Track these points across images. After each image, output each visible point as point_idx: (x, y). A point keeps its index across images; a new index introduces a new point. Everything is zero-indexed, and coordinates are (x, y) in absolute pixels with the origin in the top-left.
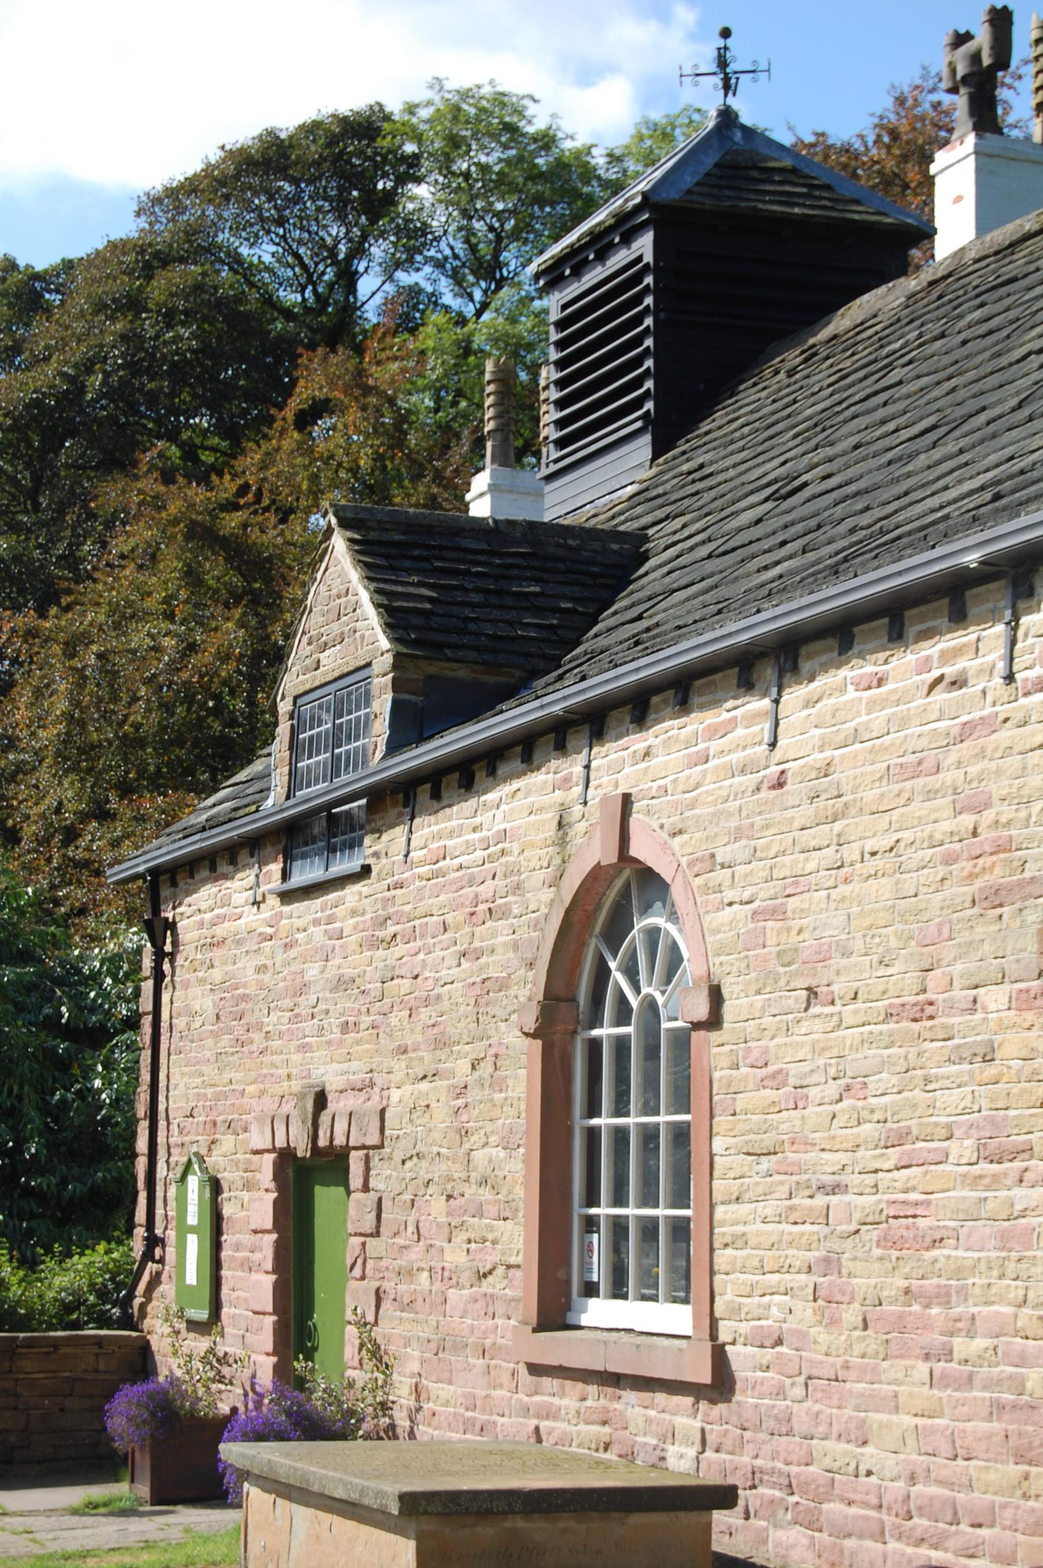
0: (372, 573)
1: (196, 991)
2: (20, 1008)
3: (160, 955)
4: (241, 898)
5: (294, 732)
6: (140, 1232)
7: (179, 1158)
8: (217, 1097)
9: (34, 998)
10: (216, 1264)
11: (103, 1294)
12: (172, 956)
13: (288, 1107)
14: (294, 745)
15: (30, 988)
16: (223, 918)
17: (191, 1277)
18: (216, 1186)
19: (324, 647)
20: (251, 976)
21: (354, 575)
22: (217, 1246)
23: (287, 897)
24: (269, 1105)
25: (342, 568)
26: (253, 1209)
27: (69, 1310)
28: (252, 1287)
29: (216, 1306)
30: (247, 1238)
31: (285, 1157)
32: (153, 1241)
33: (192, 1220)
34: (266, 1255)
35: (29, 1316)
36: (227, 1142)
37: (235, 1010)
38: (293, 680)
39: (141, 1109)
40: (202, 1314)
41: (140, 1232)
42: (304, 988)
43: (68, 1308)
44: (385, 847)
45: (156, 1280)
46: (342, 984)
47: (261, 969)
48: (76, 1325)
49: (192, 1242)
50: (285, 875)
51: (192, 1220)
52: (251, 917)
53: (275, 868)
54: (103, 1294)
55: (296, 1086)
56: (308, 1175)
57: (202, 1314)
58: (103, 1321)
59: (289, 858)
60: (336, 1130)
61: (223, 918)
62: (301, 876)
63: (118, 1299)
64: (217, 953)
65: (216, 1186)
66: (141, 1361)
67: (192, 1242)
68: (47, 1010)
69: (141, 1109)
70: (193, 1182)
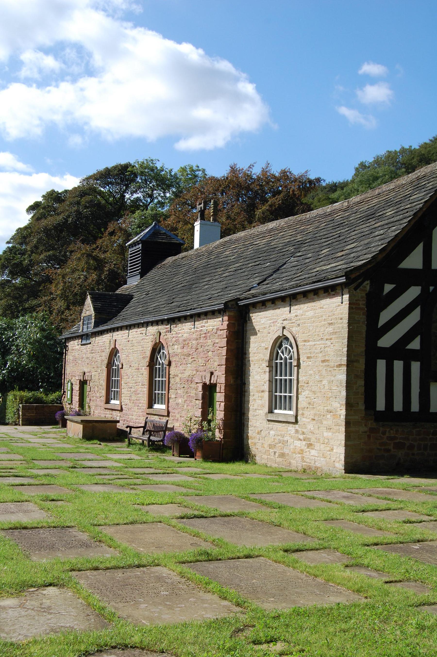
0: (93, 302)
1: (70, 356)
2: (50, 349)
3: (66, 350)
4: (76, 344)
5: (83, 322)
6: (63, 390)
7: (68, 380)
8: (73, 372)
9: (53, 347)
10: (72, 395)
11: (57, 399)
12: (68, 351)
13: (81, 374)
14: (83, 324)
15: (53, 345)
16: (74, 346)
17: (69, 397)
18: (72, 384)
19: (87, 311)
20: (77, 355)
21: (90, 302)
22: (72, 393)
23: (82, 345)
24: (78, 373)
25: (89, 301)
26: (76, 388)
27: (53, 401)
28: (76, 398)
29: (72, 401)
30: (76, 392)
31: (80, 380)
32: (64, 392)
33: (69, 389)
34: (78, 394)
35: (46, 402)
36: (74, 378)
37: (75, 360)
38: (83, 315)
39: (63, 373)
40: (70, 402)
41: (63, 390)
42: (83, 358)
43: (53, 401)
44: (93, 340)
45: (64, 397)
46: (87, 358)
47: (78, 354)
48: (53, 404)
49: (69, 392)
50: (81, 342)
51: (69, 389)
52: (77, 347)
53: (80, 340)
54: (57, 399)
55: (82, 371)
56: (83, 383)
57: (70, 402)
58: (57, 403)
59: (82, 339)
60: (86, 378)
61: (74, 346)
62: (84, 342)
63: (59, 400)
64: (73, 351)
65: (72, 384)
66: (62, 408)
67: (69, 392)
68: (56, 349)
69: (63, 373)
70: (69, 383)
